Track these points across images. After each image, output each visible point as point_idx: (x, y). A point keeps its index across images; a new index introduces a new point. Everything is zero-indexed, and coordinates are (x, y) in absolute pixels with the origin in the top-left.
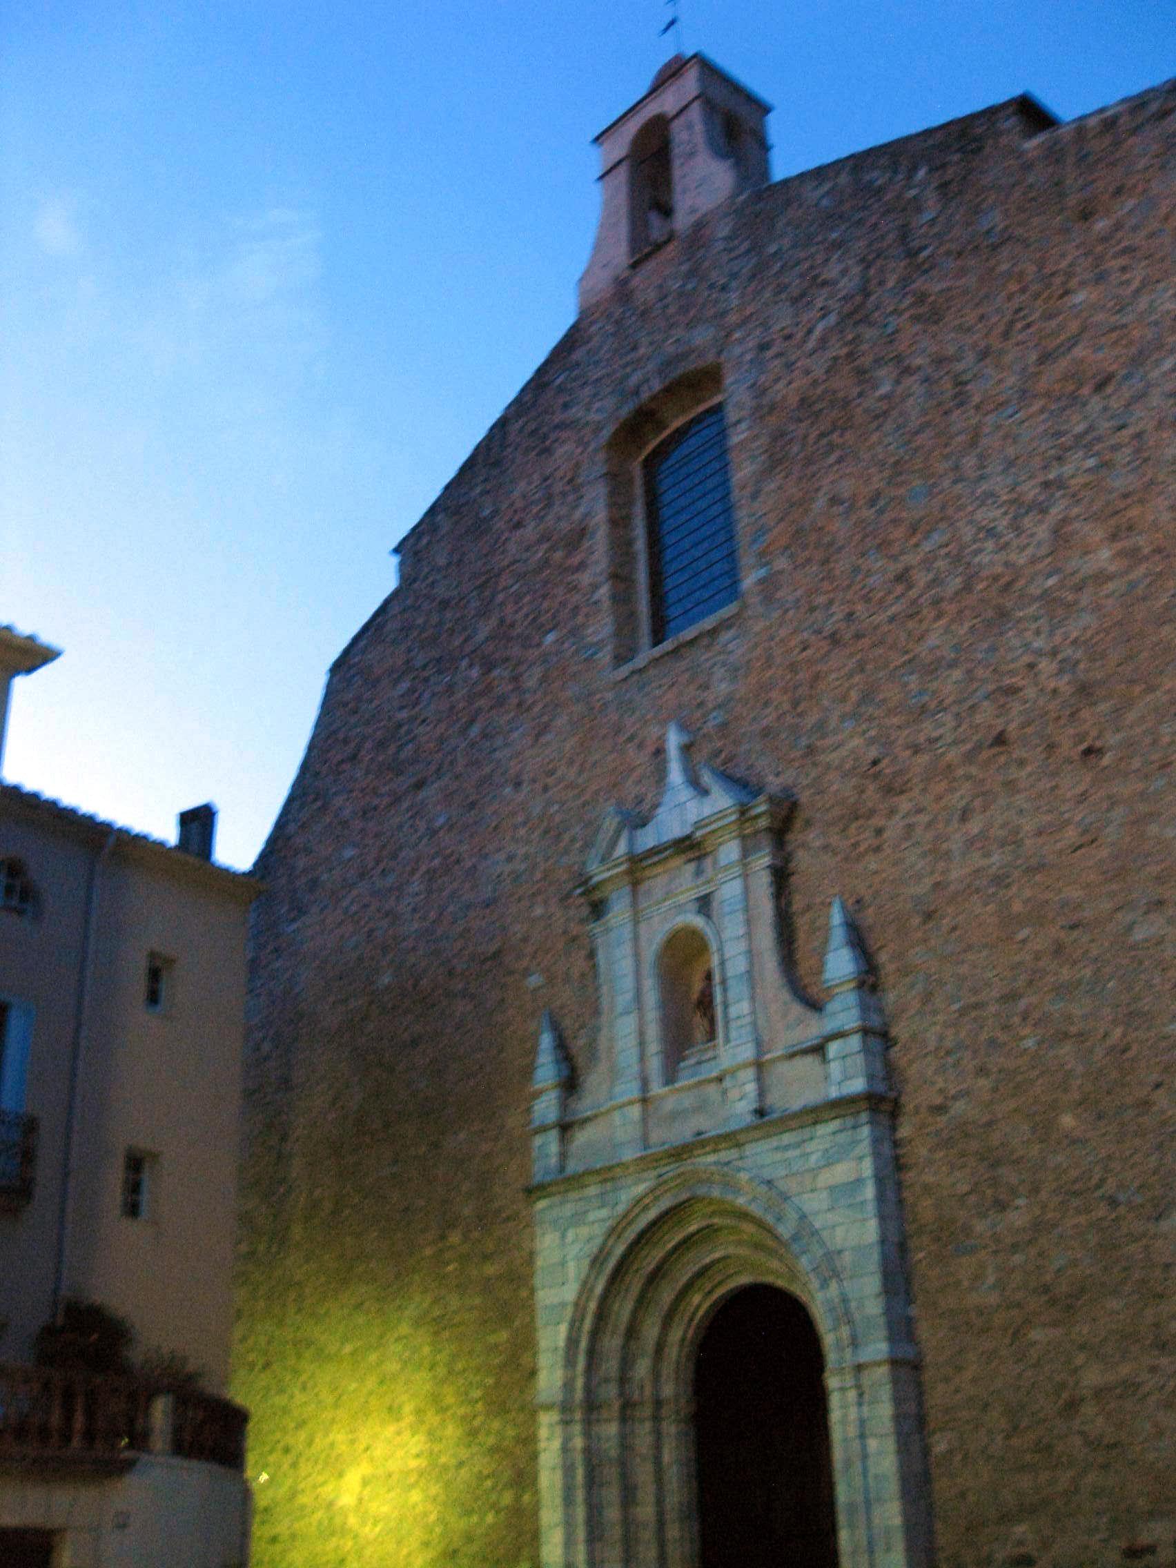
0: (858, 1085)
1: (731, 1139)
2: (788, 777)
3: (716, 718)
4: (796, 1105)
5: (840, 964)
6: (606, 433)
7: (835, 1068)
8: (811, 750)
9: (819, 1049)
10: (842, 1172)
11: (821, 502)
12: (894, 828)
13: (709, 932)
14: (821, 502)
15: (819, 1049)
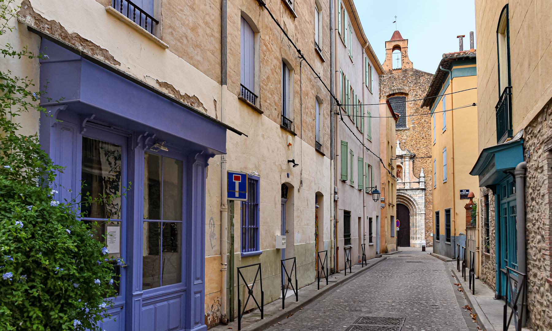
0: (424, 187)
1: (406, 190)
2: (415, 151)
3: (404, 141)
4: (414, 188)
5: (422, 175)
6: (387, 94)
7: (421, 185)
8: (418, 149)
9: (419, 182)
10: (421, 195)
11: (423, 120)
12: (428, 161)
13: (403, 167)
14: (423, 120)
15: (419, 182)
